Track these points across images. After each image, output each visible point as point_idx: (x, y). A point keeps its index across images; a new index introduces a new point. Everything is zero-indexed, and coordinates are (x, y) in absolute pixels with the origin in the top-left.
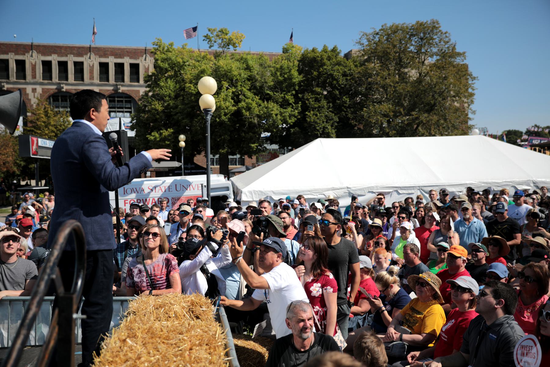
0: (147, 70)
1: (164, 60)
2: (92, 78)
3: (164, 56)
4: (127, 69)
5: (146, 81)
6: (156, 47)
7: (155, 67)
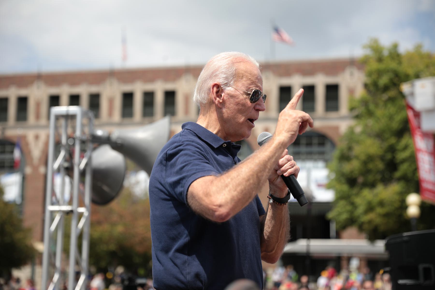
0: (351, 92)
3: (382, 66)
5: (352, 109)
7: (366, 86)
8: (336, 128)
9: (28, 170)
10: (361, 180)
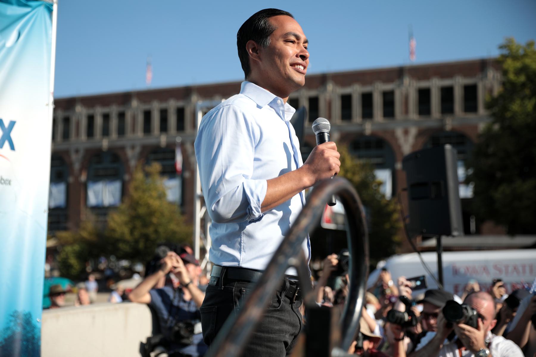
0: (491, 91)
1: (518, 72)
2: (406, 111)
3: (518, 64)
4: (458, 95)
6: (505, 52)
7: (504, 84)
8: (476, 127)
10: (499, 175)
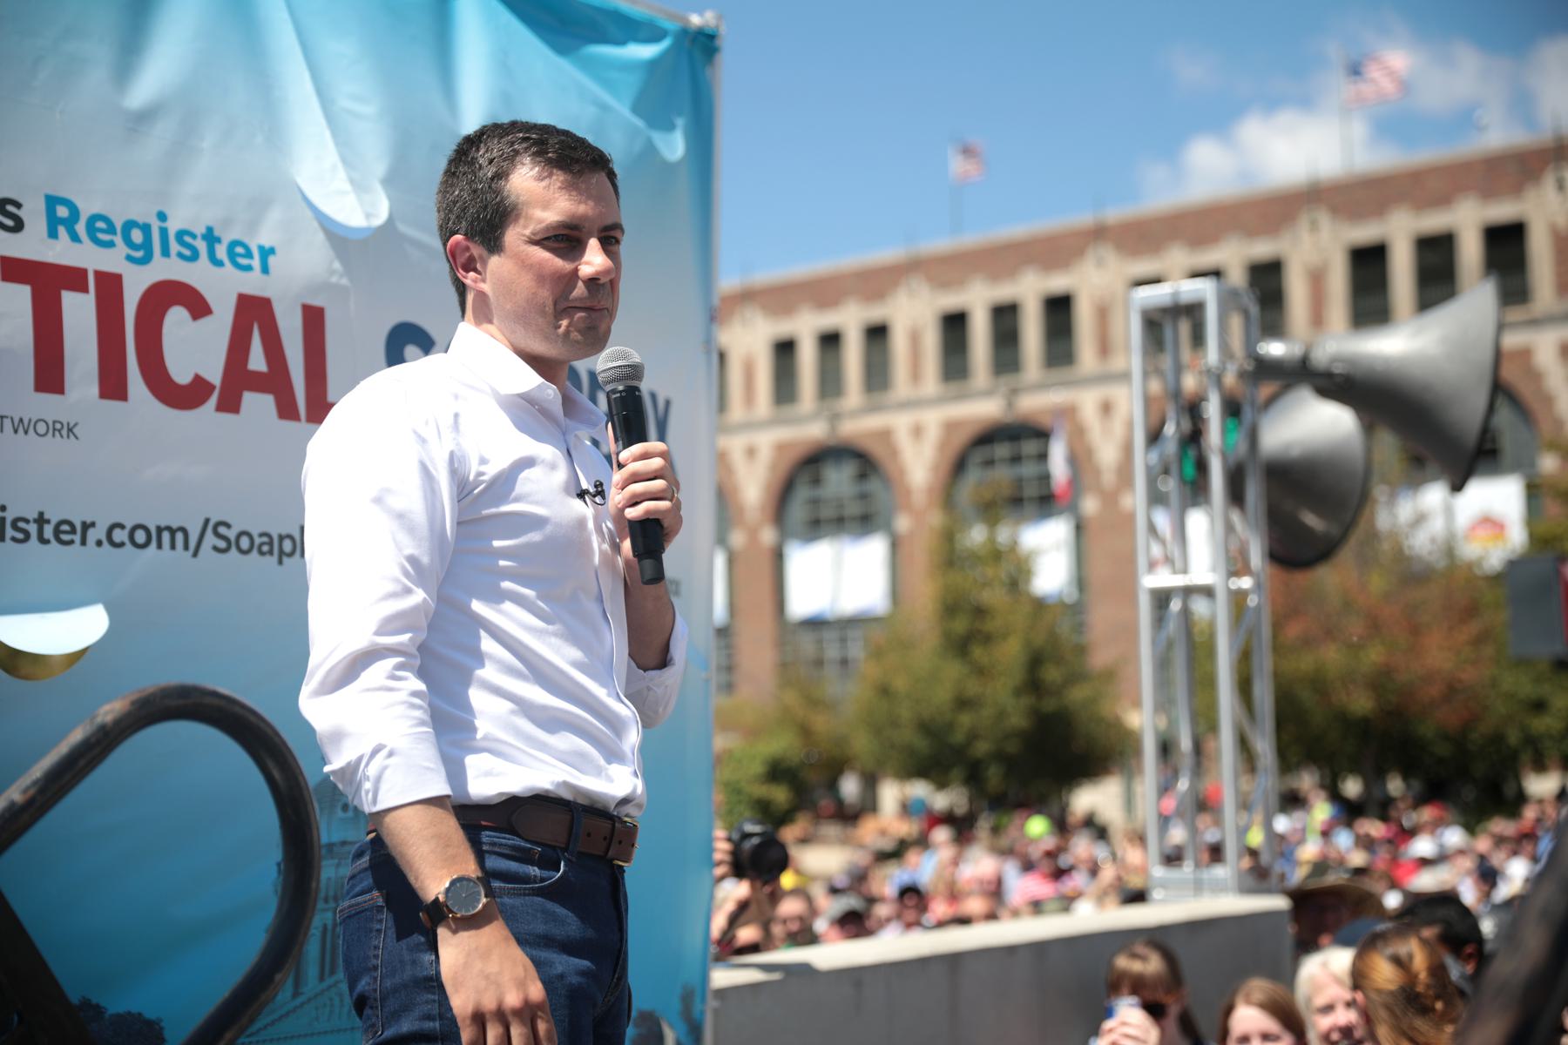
9: (1090, 505)
